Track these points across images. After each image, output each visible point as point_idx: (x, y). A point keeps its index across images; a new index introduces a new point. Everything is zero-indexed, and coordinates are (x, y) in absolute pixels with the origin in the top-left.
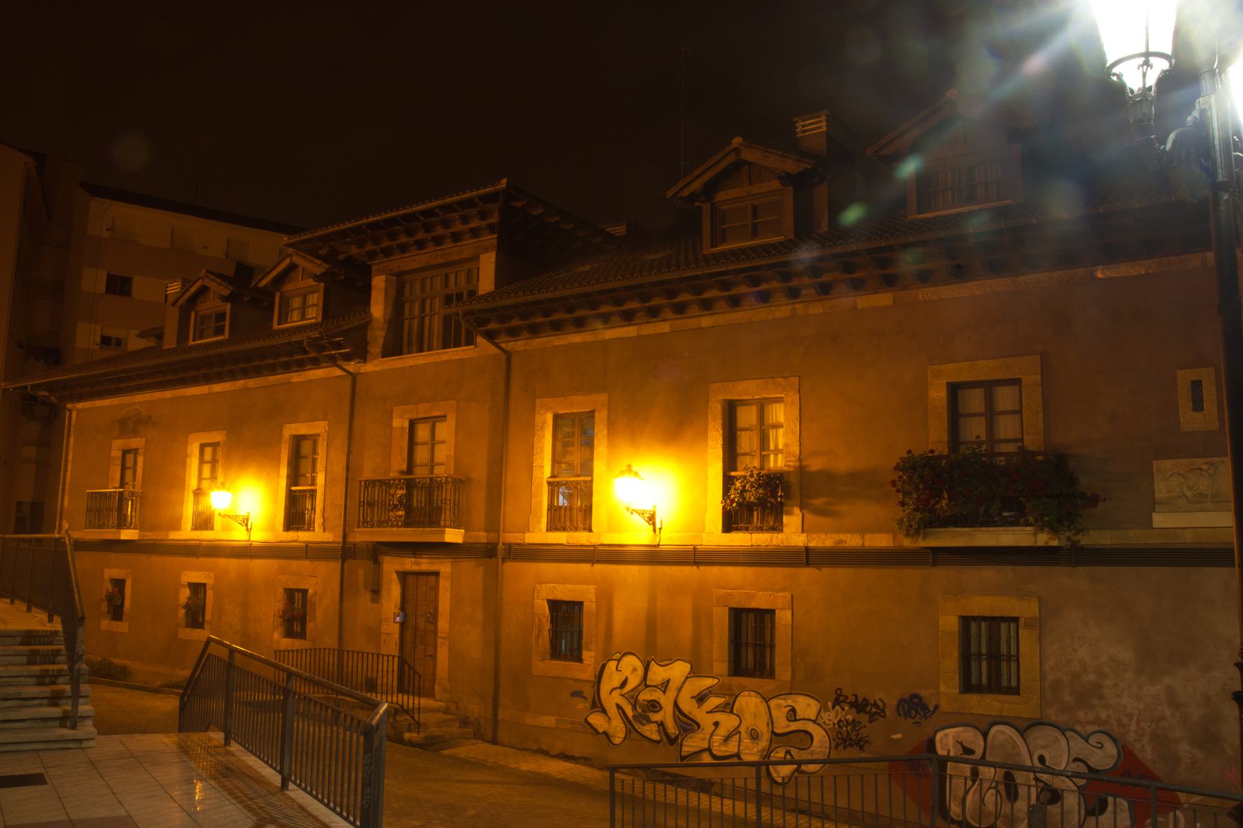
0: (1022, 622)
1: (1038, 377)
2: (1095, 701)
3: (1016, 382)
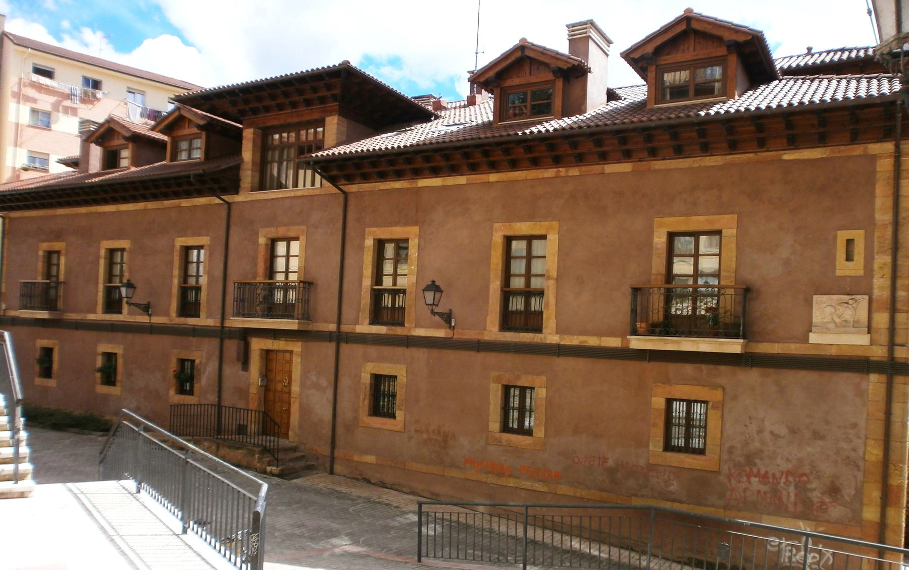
0: (710, 405)
1: (735, 231)
2: (757, 461)
3: (719, 233)
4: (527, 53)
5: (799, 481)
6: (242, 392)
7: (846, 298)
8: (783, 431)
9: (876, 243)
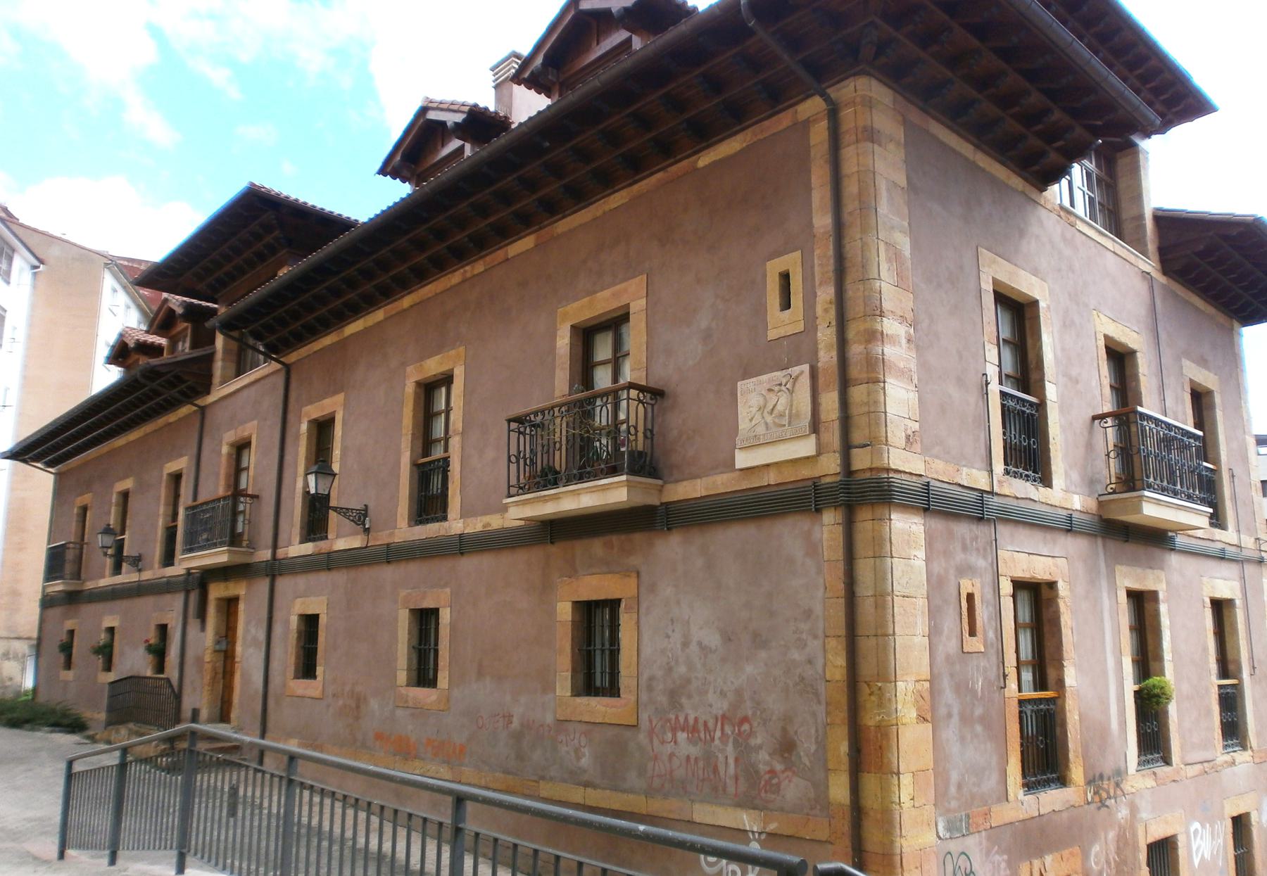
1: (644, 301)
2: (684, 700)
4: (432, 115)
5: (740, 733)
6: (199, 661)
7: (778, 375)
8: (714, 640)
9: (817, 269)
